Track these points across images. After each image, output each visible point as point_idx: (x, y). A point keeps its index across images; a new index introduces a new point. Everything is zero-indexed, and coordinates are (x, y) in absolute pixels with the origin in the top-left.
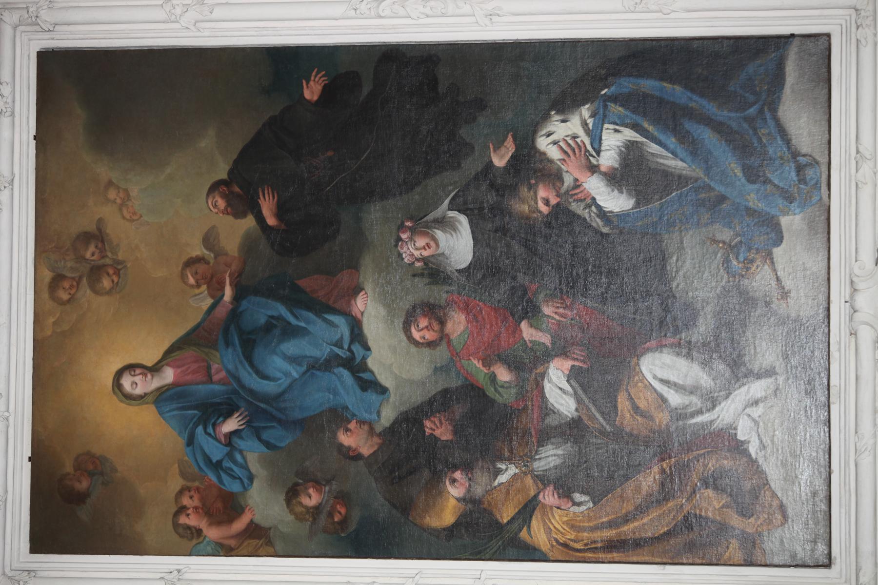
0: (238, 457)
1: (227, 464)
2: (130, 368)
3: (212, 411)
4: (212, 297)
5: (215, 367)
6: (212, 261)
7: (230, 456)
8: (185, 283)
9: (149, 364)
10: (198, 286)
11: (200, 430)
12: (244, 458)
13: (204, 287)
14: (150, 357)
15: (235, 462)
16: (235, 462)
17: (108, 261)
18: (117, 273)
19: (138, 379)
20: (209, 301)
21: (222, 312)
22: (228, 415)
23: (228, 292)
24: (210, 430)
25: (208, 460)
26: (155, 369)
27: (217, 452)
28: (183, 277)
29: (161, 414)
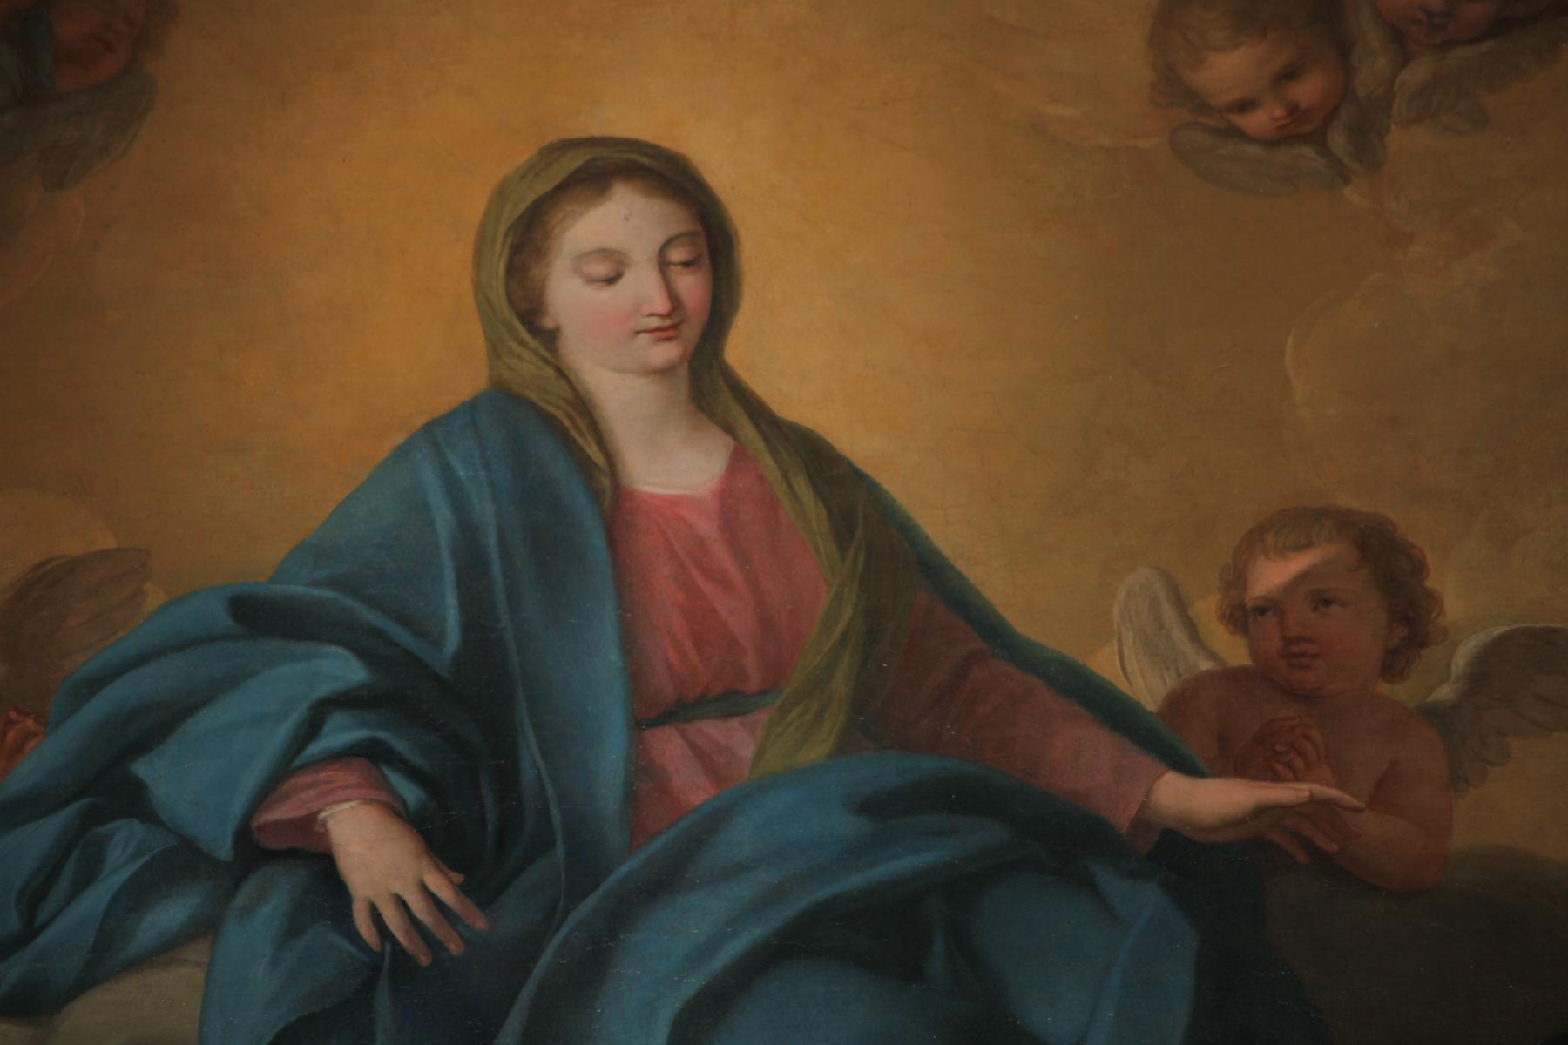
0: (171, 913)
1: (125, 848)
2: (711, 239)
3: (461, 737)
4: (1177, 703)
5: (739, 740)
6: (1402, 692)
7: (181, 861)
8: (1256, 540)
9: (738, 350)
10: (1240, 617)
11: (342, 669)
12: (167, 949)
13: (1235, 652)
14: (774, 351)
15: (139, 894)
16: (139, 894)
17: (1372, 66)
18: (1302, 129)
19: (643, 288)
20: (1147, 689)
21: (1085, 765)
22: (439, 834)
23: (1207, 799)
24: (340, 733)
25: (153, 726)
26: (706, 383)
27: (201, 782)
28: (1295, 522)
29: (434, 433)
